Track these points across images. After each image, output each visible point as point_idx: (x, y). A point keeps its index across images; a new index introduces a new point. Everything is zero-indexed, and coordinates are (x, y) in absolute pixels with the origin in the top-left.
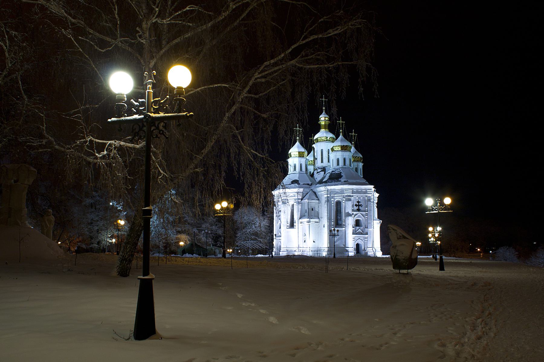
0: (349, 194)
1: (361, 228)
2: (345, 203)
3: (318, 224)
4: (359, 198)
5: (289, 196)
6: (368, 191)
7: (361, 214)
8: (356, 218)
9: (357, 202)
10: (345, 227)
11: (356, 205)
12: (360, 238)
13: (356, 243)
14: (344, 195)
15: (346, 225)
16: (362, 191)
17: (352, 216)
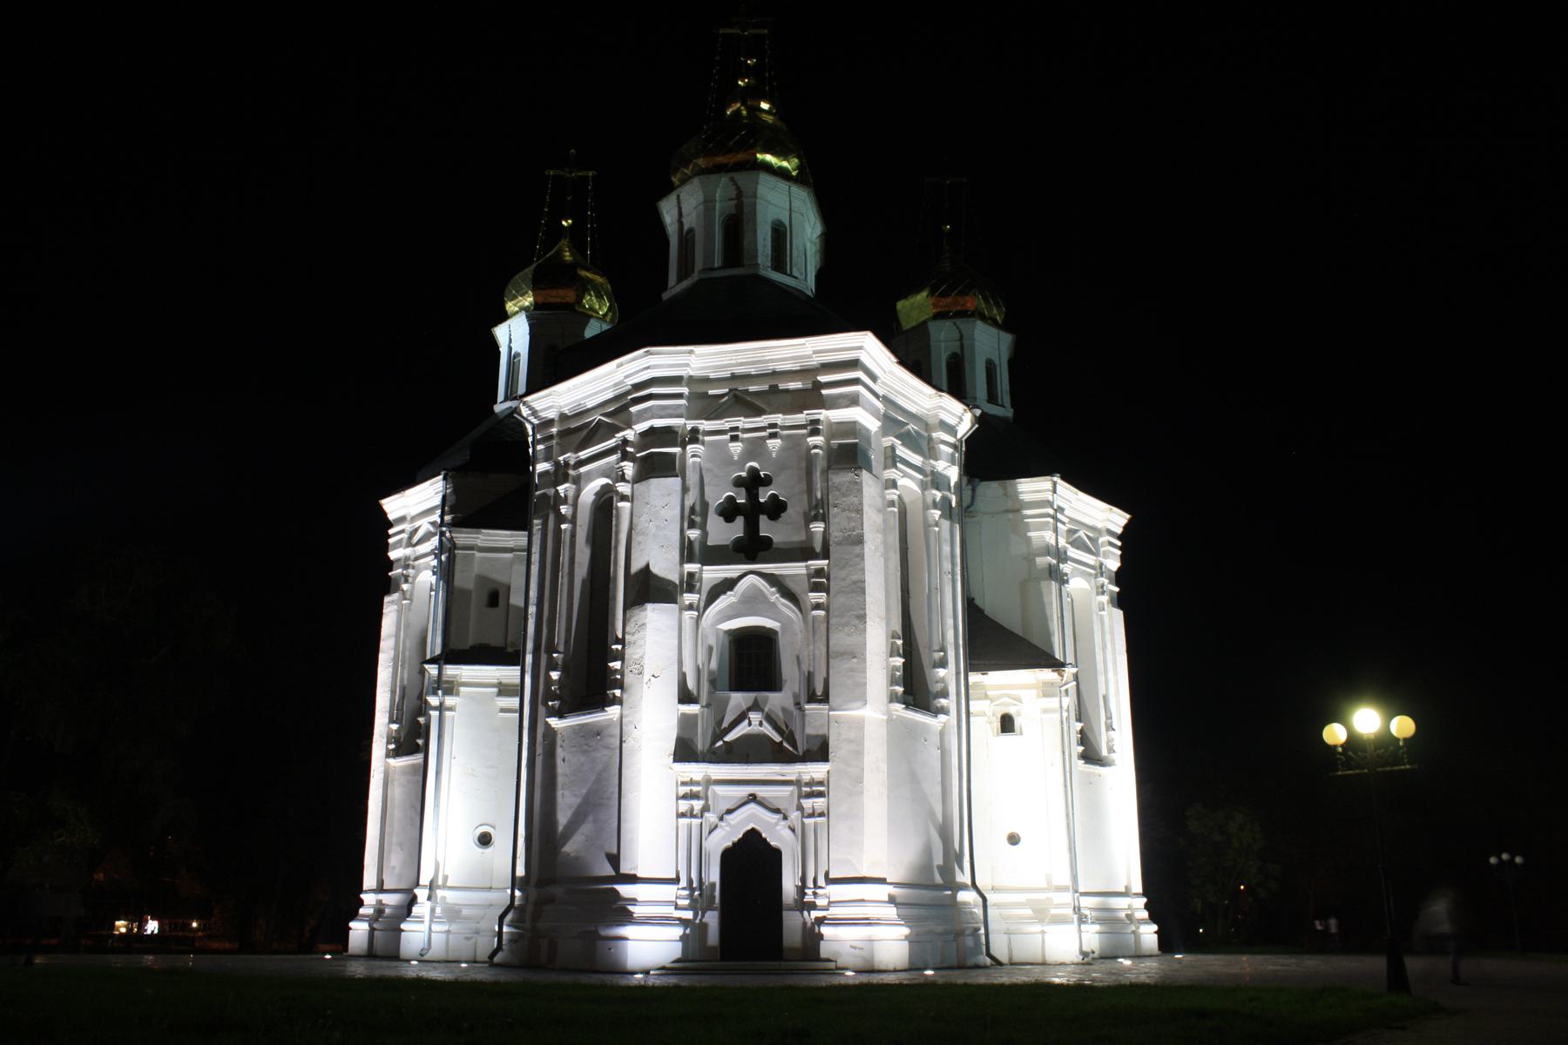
1: (776, 701)
4: (755, 448)
5: (415, 539)
6: (823, 379)
9: (738, 482)
12: (761, 791)
15: (629, 679)
16: (774, 389)
17: (674, 601)
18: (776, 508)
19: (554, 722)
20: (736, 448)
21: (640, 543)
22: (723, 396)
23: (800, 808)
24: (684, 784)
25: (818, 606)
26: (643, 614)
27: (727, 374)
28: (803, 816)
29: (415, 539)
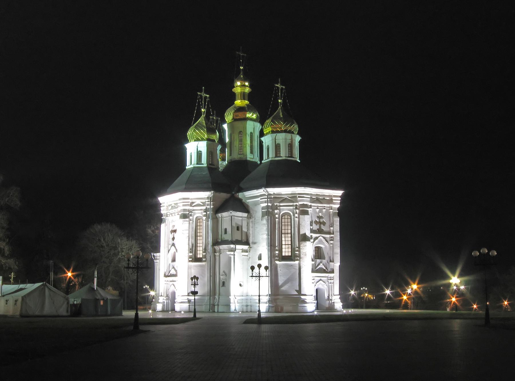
0: (305, 203)
1: (324, 261)
2: (299, 218)
3: (246, 254)
5: (193, 205)
6: (334, 198)
7: (322, 236)
8: (316, 244)
10: (299, 260)
11: (316, 222)
12: (322, 278)
13: (316, 287)
14: (296, 205)
15: (302, 256)
16: (324, 198)
17: (310, 241)
18: (324, 224)
19: (277, 262)
20: (318, 210)
21: (303, 228)
22: (315, 198)
23: (328, 282)
24: (313, 277)
25: (331, 244)
26: (306, 243)
27: (316, 194)
28: (328, 283)
29: (193, 205)
